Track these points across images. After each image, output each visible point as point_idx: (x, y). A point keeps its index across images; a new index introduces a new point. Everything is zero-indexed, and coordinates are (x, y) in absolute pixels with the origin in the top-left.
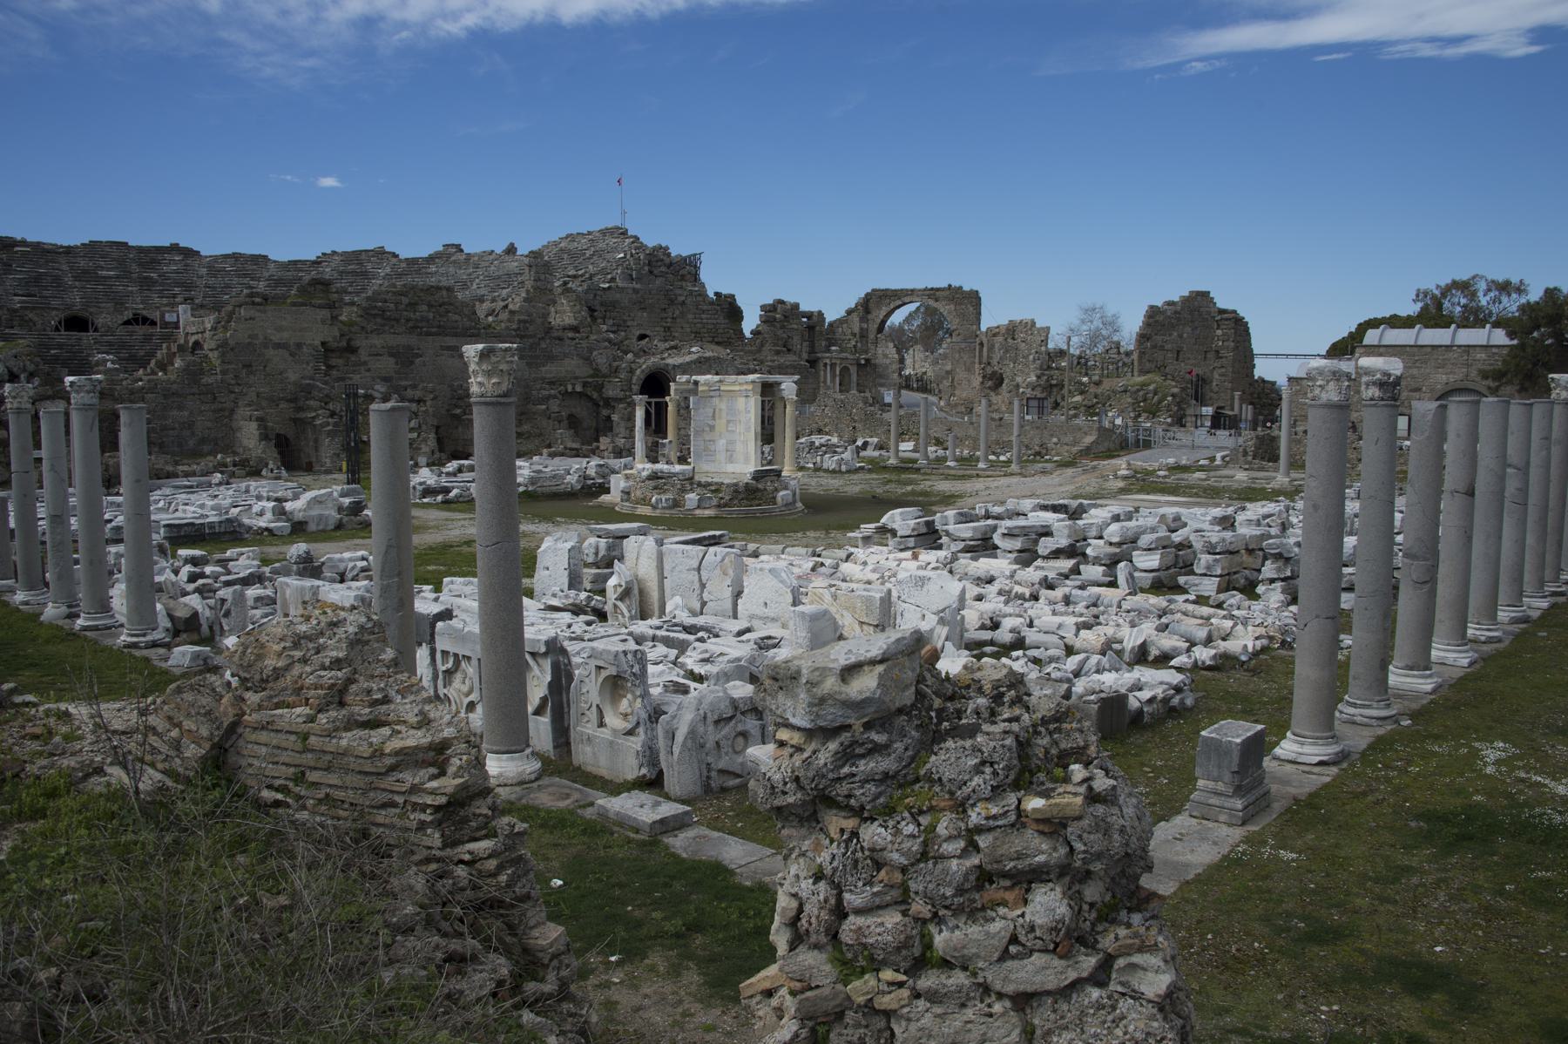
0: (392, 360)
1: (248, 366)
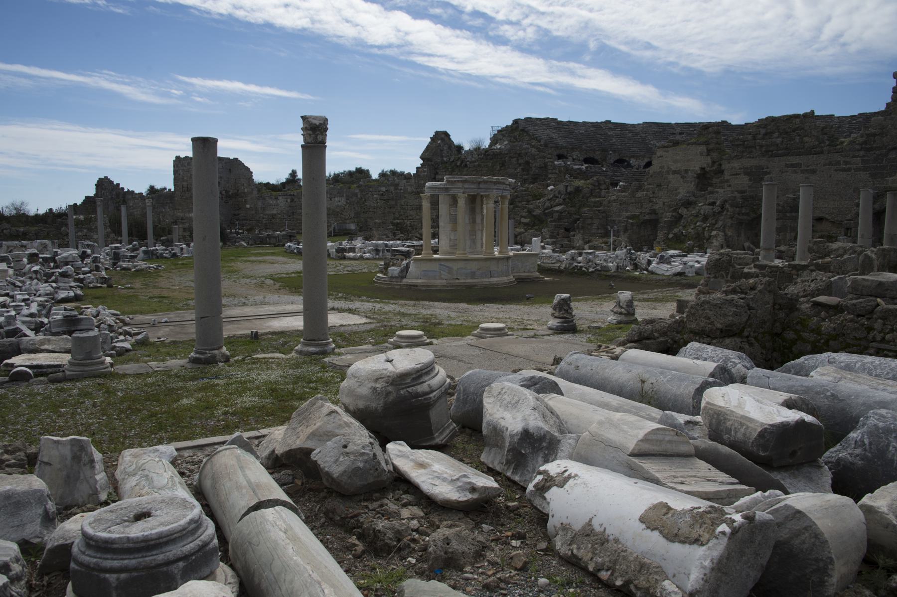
0: (747, 178)
1: (659, 186)
